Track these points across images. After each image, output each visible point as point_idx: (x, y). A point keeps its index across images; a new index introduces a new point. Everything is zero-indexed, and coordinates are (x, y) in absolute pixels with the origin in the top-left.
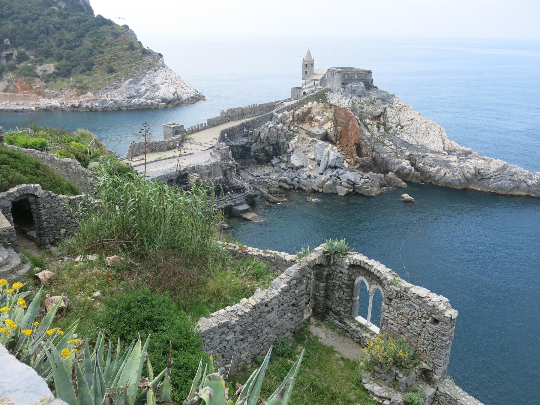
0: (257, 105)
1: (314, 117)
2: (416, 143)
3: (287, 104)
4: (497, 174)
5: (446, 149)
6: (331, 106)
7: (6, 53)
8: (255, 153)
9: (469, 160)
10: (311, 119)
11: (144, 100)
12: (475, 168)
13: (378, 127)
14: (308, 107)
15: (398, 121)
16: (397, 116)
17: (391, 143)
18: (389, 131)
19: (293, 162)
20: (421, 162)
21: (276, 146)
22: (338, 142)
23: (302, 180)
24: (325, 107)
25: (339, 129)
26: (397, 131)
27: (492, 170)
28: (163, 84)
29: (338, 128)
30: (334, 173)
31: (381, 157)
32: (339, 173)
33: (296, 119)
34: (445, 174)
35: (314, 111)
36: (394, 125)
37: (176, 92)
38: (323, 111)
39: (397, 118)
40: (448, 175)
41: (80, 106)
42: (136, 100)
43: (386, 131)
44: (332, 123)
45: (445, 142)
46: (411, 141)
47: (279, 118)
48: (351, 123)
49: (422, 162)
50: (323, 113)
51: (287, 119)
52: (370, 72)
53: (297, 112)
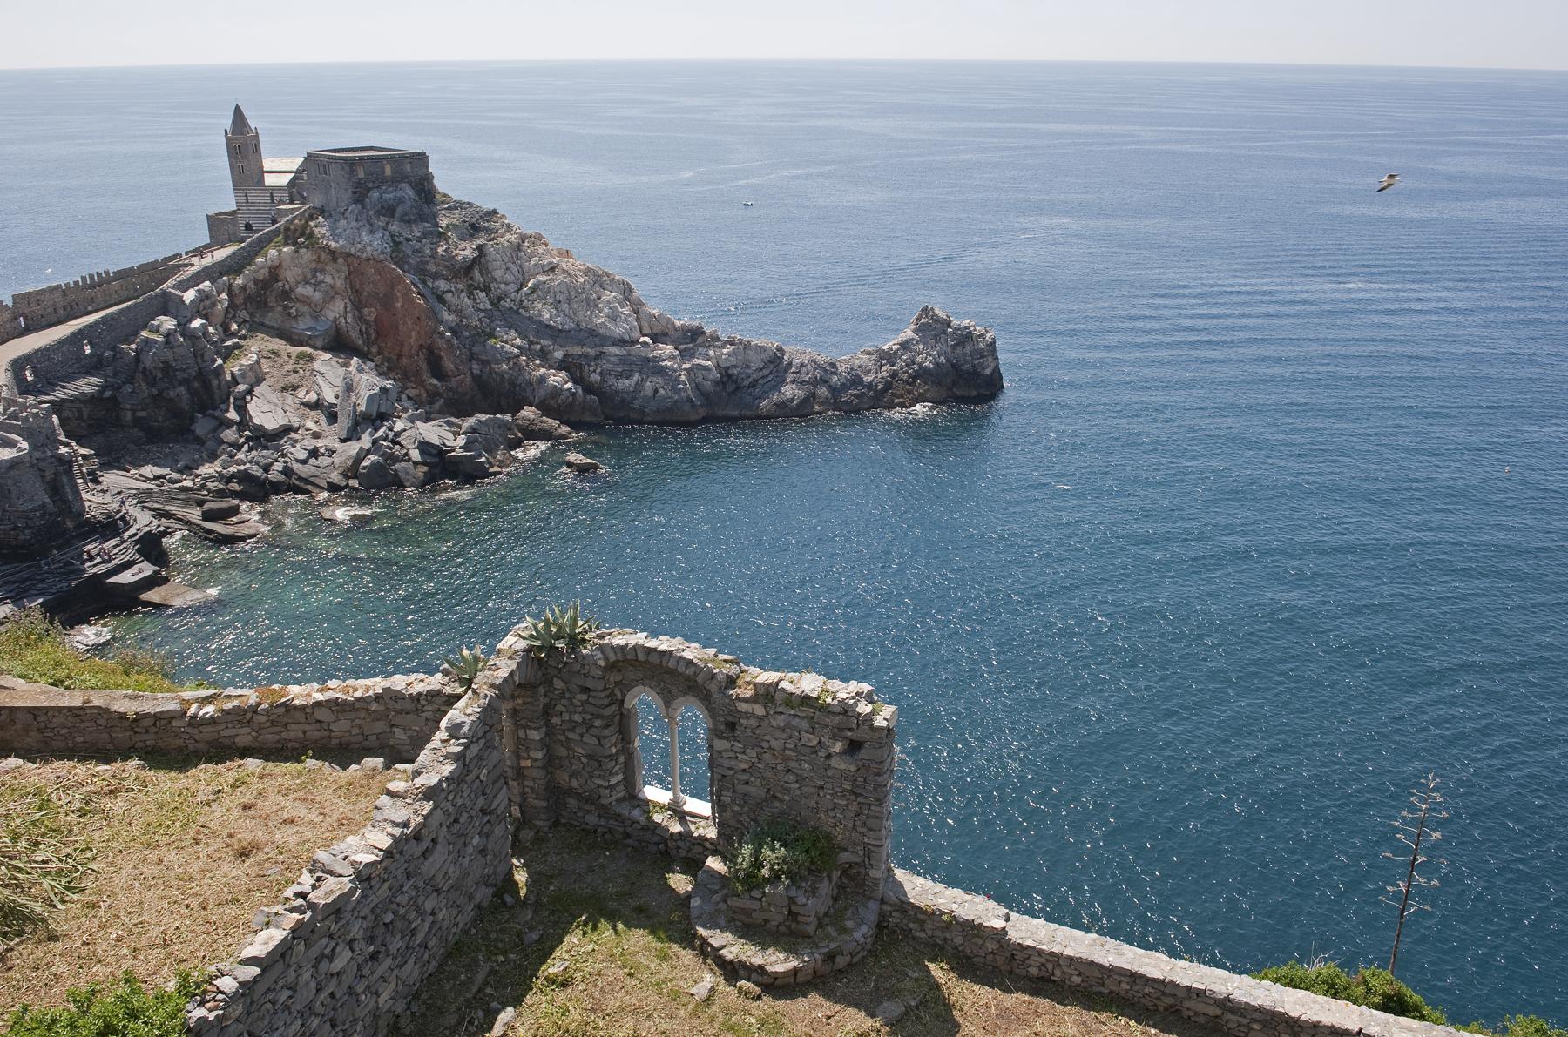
0: (107, 273)
1: (292, 290)
2: (573, 326)
3: (200, 263)
4: (765, 372)
8: (134, 412)
9: (700, 350)
10: (286, 295)
12: (718, 366)
13: (470, 294)
14: (269, 263)
15: (520, 276)
16: (514, 263)
17: (512, 333)
18: (502, 302)
19: (257, 421)
20: (594, 371)
21: (196, 384)
22: (374, 350)
23: (296, 466)
24: (319, 258)
25: (370, 313)
26: (522, 301)
29: (366, 311)
30: (380, 433)
31: (496, 373)
32: (395, 430)
33: (240, 300)
34: (656, 391)
35: (290, 274)
36: (512, 287)
38: (316, 271)
39: (514, 269)
40: (662, 392)
44: (347, 300)
45: (641, 315)
47: (187, 302)
48: (399, 294)
49: (598, 371)
50: (315, 276)
51: (214, 305)
52: (421, 158)
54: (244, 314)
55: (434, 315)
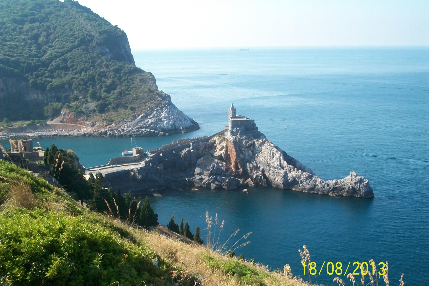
7: (65, 94)
11: (149, 130)
41: (106, 133)
42: (144, 129)
52: (254, 120)
54: (207, 150)
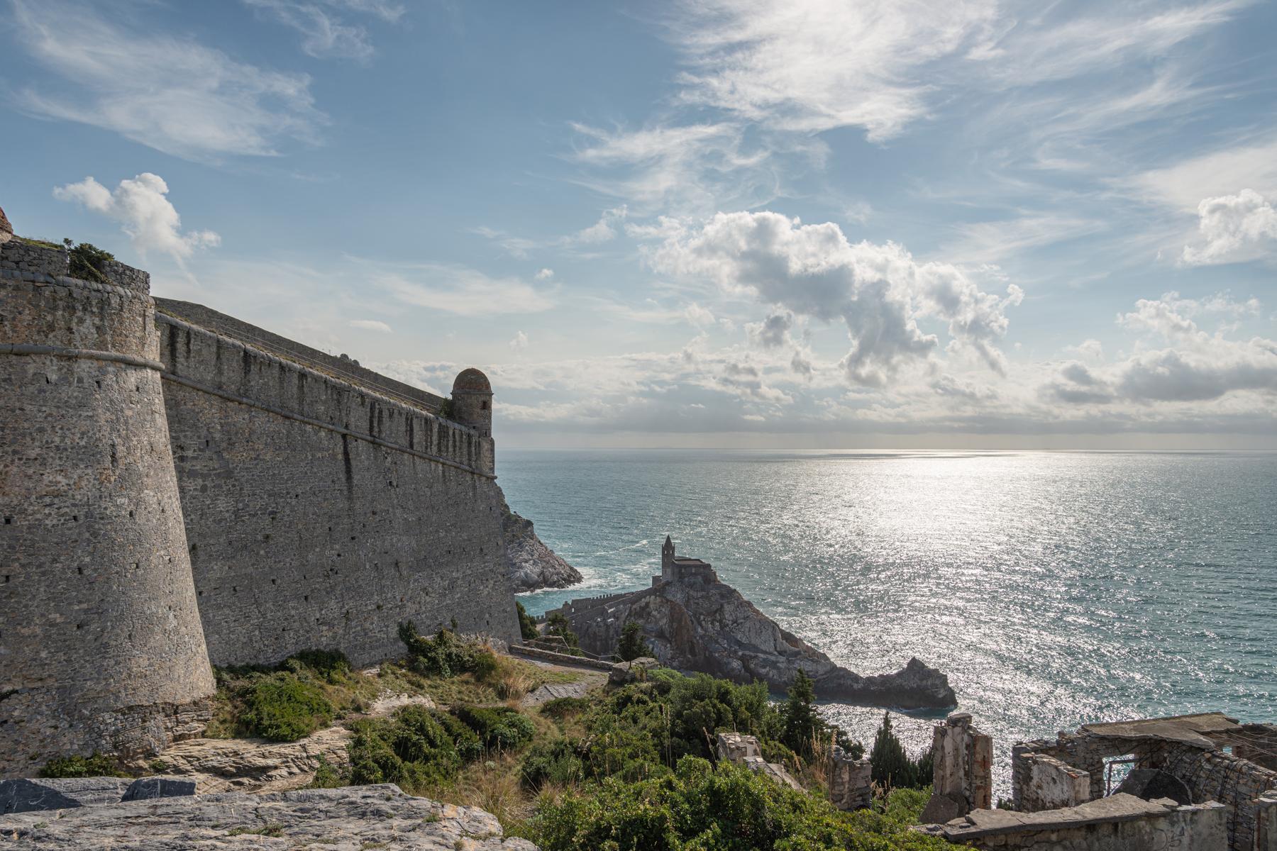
4: (825, 676)
5: (778, 649)
6: (668, 601)
10: (649, 614)
27: (820, 672)
28: (526, 562)
35: (652, 606)
36: (730, 623)
37: (542, 573)
43: (722, 628)
46: (744, 640)
53: (634, 607)
55: (695, 629)
